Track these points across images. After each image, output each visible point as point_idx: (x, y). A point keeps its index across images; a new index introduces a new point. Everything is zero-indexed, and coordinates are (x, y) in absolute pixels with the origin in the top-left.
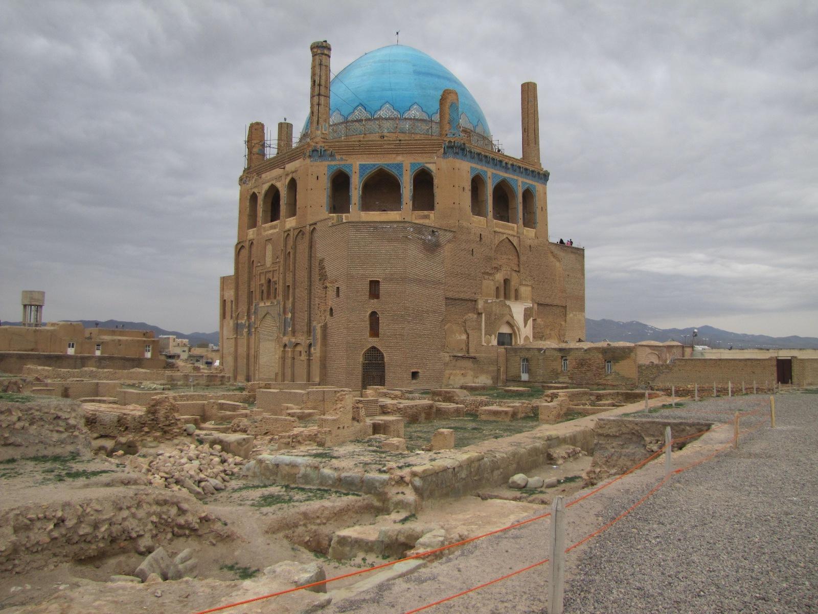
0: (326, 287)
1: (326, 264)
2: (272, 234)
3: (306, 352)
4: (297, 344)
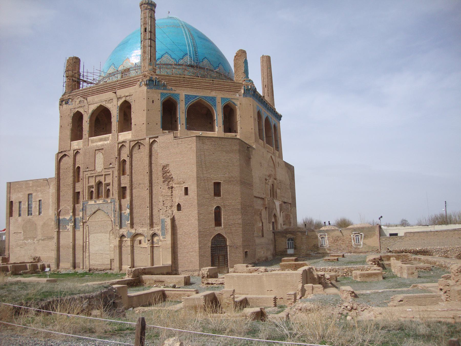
0: (172, 188)
1: (171, 168)
2: (103, 145)
3: (149, 241)
4: (137, 235)
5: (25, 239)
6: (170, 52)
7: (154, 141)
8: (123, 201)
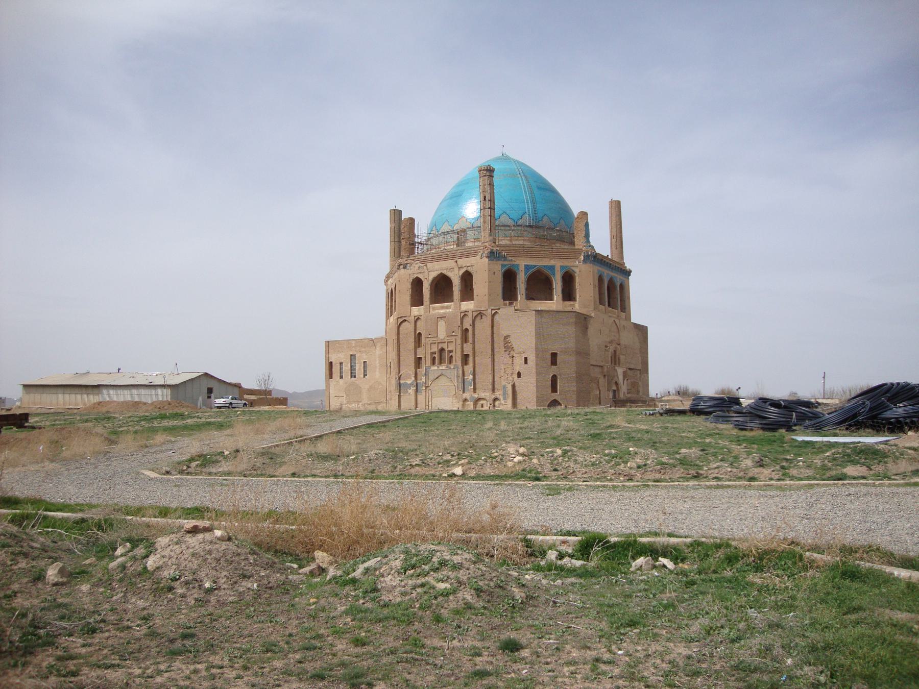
1: (512, 339)
4: (480, 399)
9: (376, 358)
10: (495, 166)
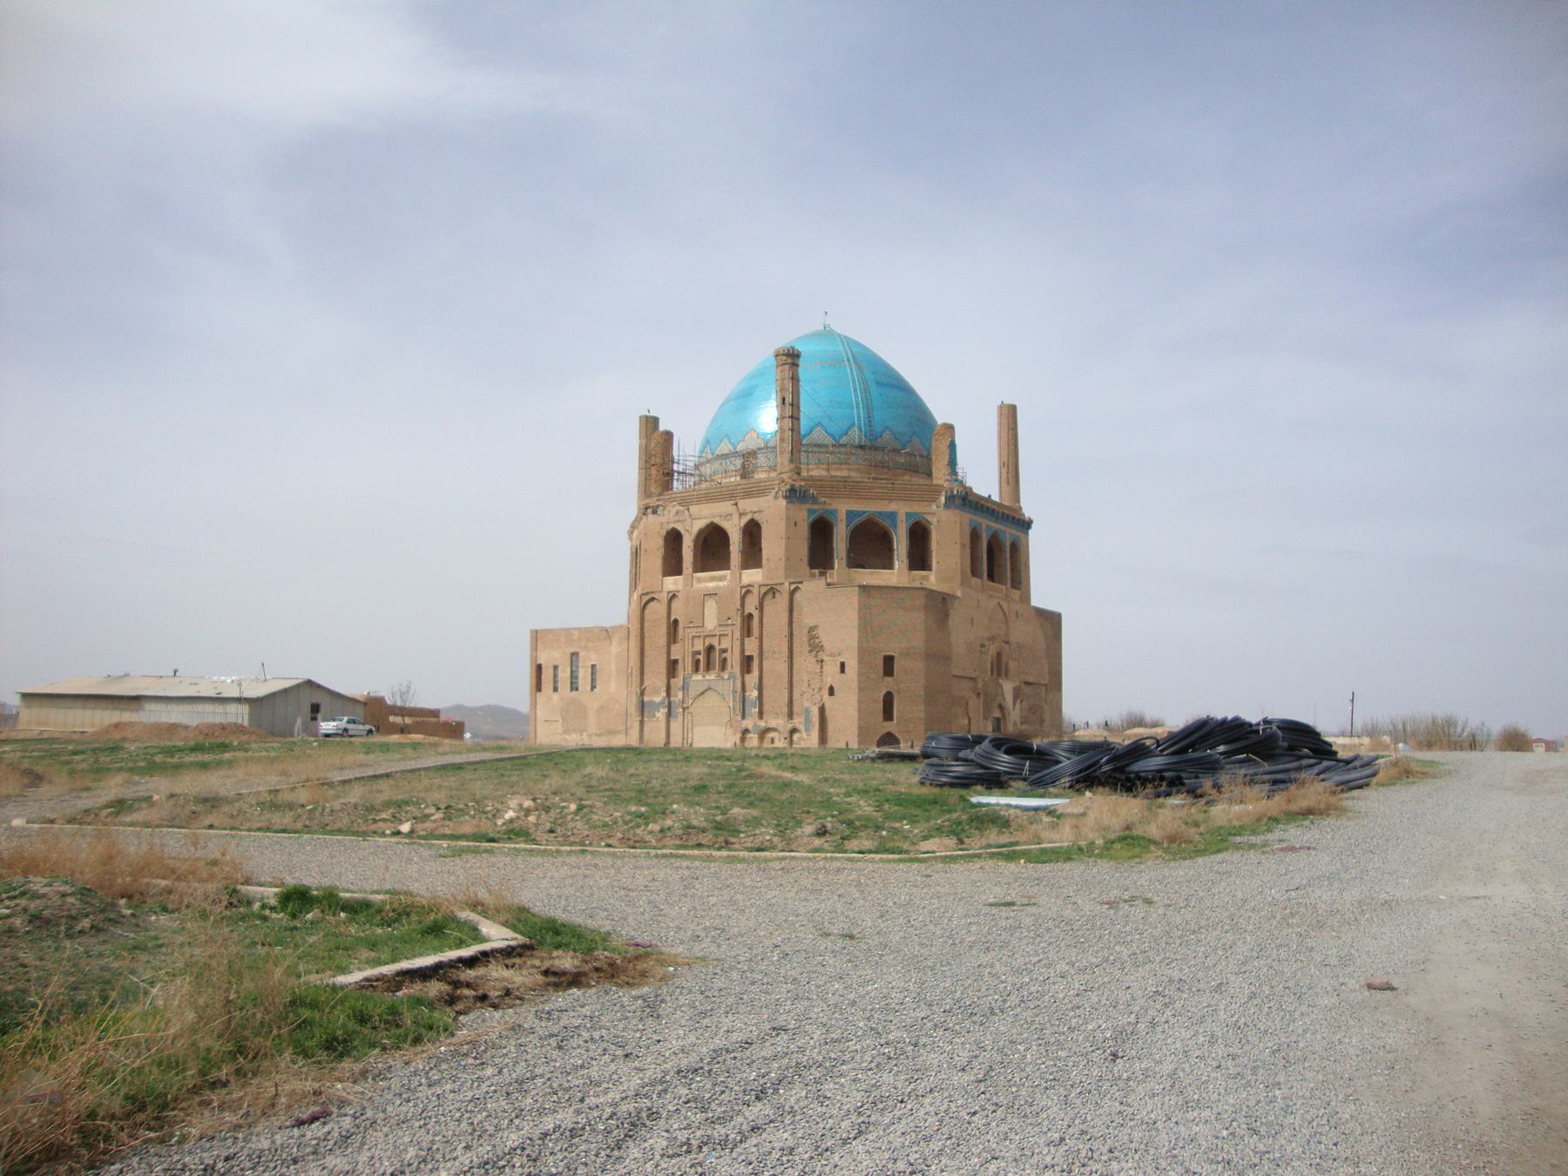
1: (820, 632)
2: (717, 588)
4: (768, 730)
5: (565, 732)
6: (825, 422)
7: (797, 589)
8: (747, 677)
9: (614, 659)
10: (800, 348)
